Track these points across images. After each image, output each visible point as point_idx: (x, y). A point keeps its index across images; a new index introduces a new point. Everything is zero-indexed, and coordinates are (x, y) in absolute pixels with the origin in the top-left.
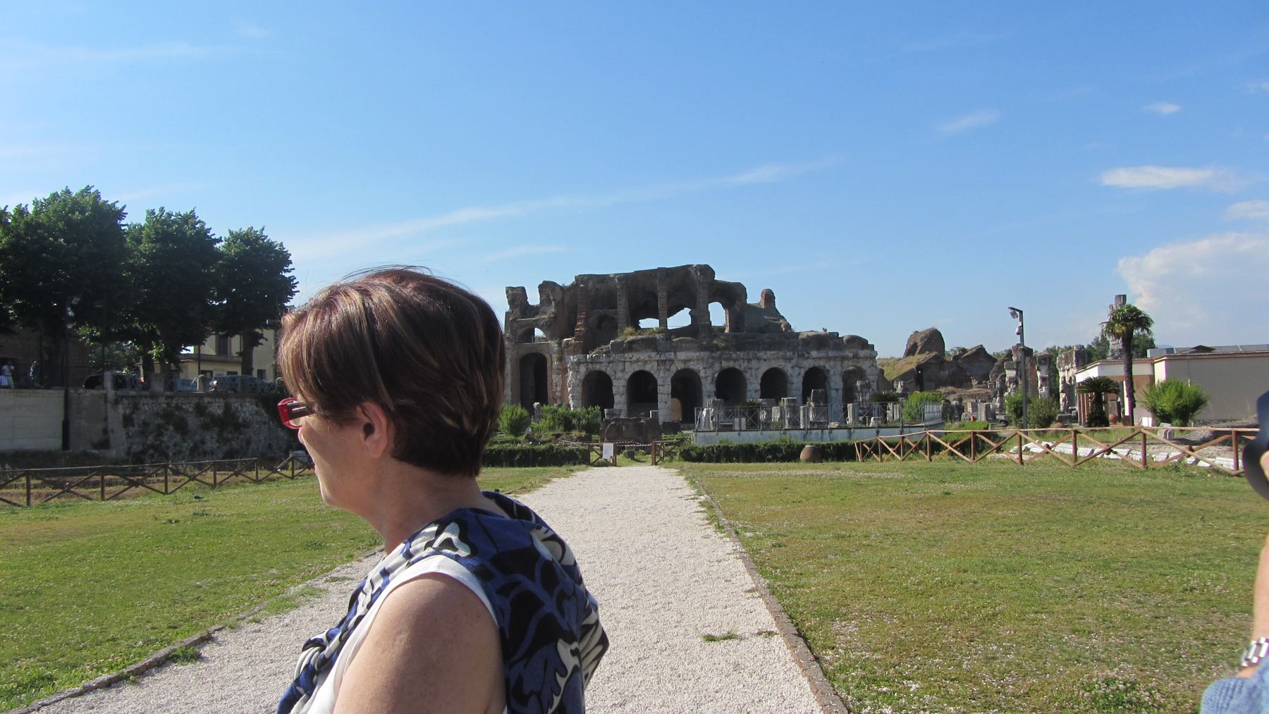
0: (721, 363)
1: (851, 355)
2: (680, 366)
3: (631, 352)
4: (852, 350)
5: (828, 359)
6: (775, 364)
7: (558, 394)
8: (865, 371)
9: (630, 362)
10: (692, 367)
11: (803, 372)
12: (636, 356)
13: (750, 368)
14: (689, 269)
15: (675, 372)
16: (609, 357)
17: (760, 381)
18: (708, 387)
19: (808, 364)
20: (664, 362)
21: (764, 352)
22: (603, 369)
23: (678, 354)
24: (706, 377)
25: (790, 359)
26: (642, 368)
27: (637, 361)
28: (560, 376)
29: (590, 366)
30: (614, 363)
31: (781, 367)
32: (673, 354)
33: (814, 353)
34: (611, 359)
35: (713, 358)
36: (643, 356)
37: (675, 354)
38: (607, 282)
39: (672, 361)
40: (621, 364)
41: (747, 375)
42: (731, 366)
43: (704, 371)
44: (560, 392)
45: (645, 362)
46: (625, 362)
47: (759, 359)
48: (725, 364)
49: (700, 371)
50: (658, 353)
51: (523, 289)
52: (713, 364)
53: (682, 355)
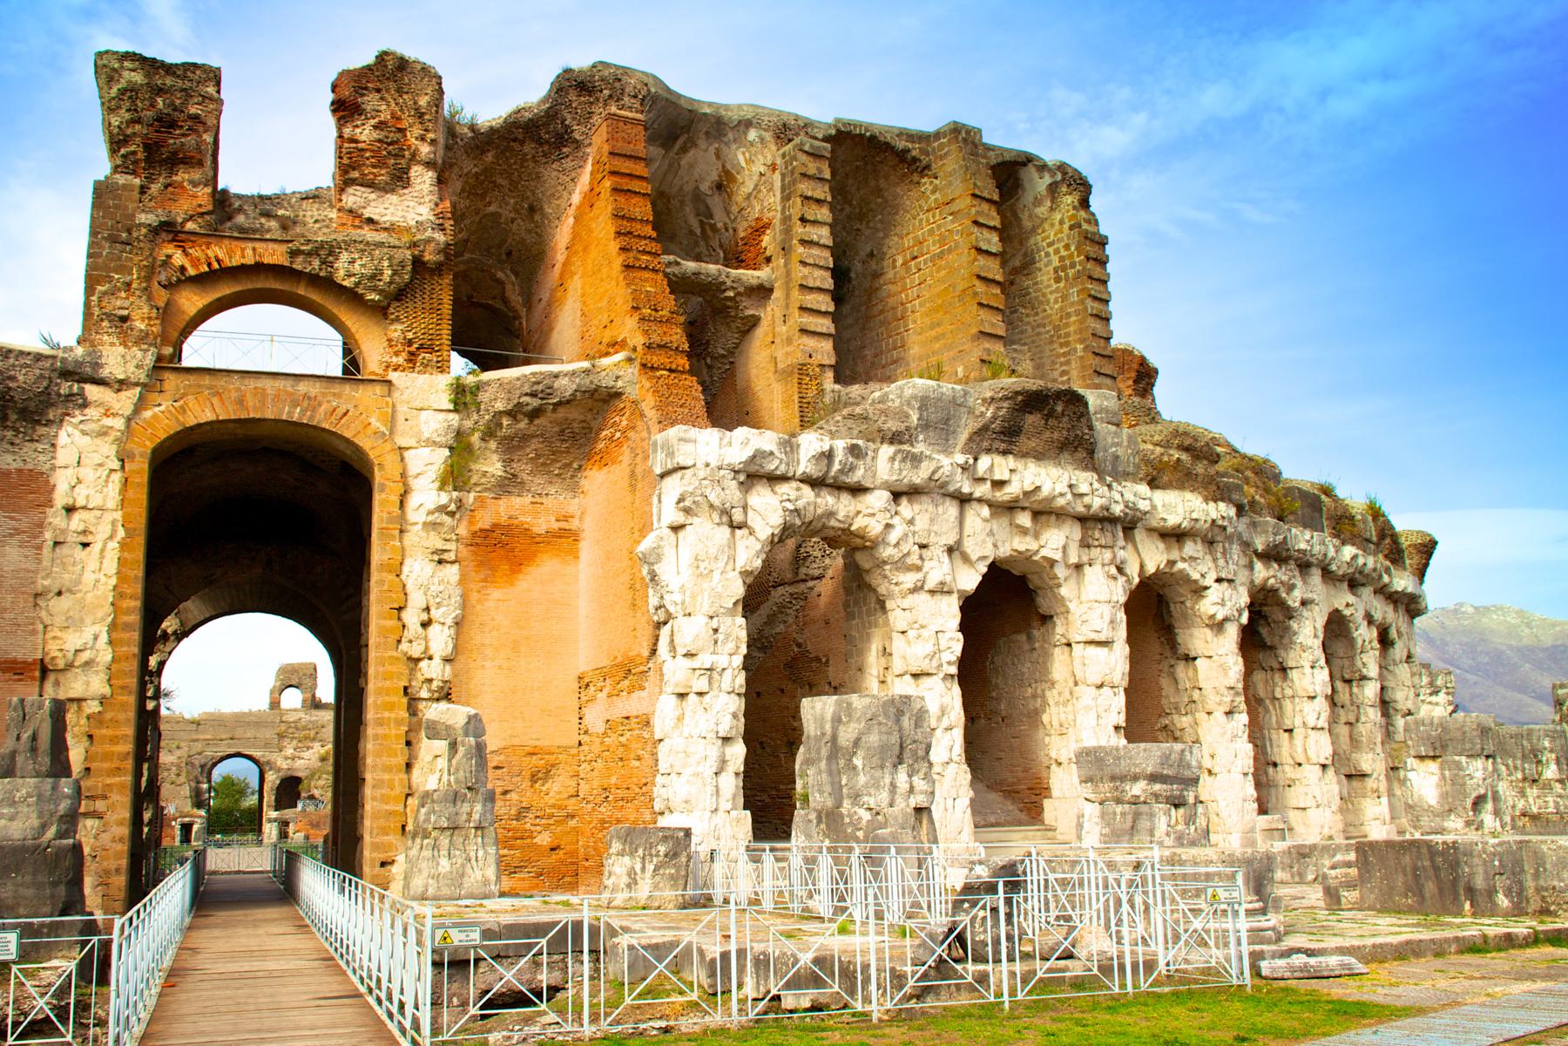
0: (1251, 567)
2: (1154, 557)
3: (1005, 453)
7: (433, 670)
20: (1104, 520)
22: (875, 528)
26: (1022, 544)
28: (452, 572)
31: (1347, 612)
34: (919, 476)
40: (951, 509)
44: (447, 660)
45: (1045, 513)
46: (964, 500)
51: (215, 76)
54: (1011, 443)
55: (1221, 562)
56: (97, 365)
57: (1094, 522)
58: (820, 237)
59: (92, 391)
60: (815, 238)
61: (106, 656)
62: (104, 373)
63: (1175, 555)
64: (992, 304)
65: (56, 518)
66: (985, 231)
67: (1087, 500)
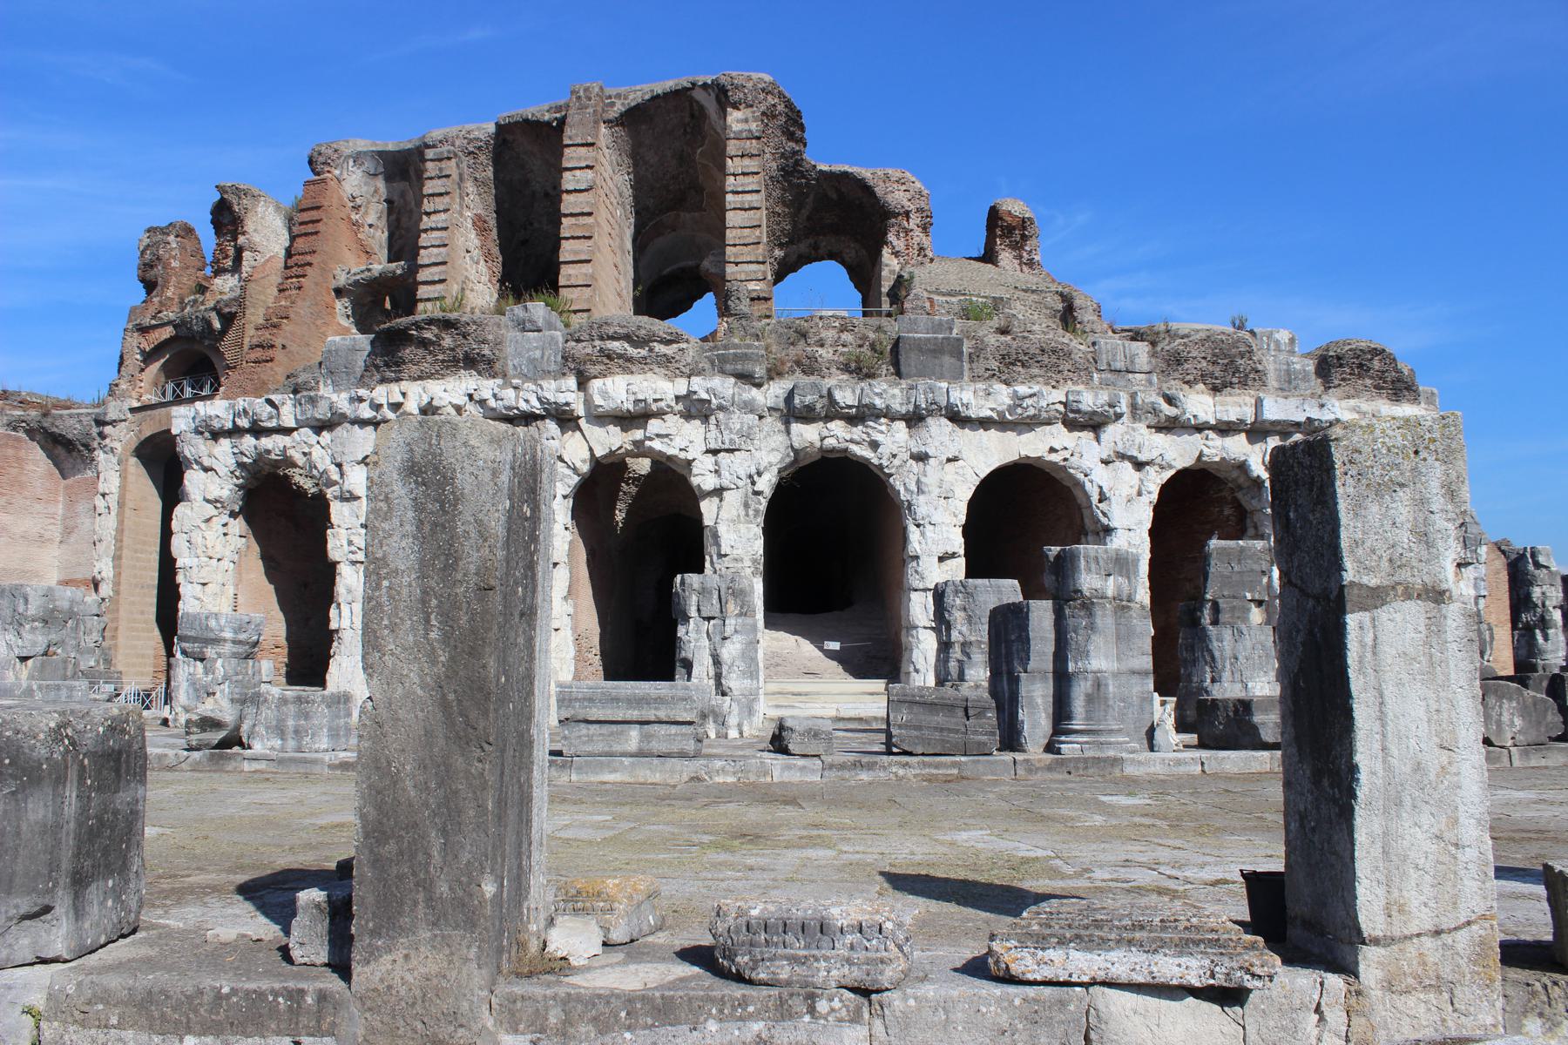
0: (788, 432)
2: (608, 440)
3: (398, 380)
4: (1352, 402)
11: (1155, 481)
13: (921, 458)
14: (699, 95)
15: (585, 468)
16: (313, 401)
17: (962, 519)
19: (1179, 452)
21: (981, 386)
23: (596, 384)
24: (719, 492)
25: (1094, 424)
29: (248, 442)
30: (339, 431)
31: (1054, 458)
32: (572, 382)
33: (1200, 404)
34: (322, 412)
35: (749, 407)
37: (582, 384)
41: (902, 483)
42: (830, 442)
43: (710, 459)
46: (375, 424)
47: (957, 418)
48: (808, 434)
49: (689, 463)
50: (507, 384)
52: (747, 435)
53: (616, 390)
54: (400, 372)
55: (714, 432)
56: (105, 414)
58: (438, 222)
59: (108, 429)
60: (434, 226)
61: (111, 575)
62: (108, 419)
63: (638, 434)
64: (576, 235)
66: (578, 173)
67: (492, 403)
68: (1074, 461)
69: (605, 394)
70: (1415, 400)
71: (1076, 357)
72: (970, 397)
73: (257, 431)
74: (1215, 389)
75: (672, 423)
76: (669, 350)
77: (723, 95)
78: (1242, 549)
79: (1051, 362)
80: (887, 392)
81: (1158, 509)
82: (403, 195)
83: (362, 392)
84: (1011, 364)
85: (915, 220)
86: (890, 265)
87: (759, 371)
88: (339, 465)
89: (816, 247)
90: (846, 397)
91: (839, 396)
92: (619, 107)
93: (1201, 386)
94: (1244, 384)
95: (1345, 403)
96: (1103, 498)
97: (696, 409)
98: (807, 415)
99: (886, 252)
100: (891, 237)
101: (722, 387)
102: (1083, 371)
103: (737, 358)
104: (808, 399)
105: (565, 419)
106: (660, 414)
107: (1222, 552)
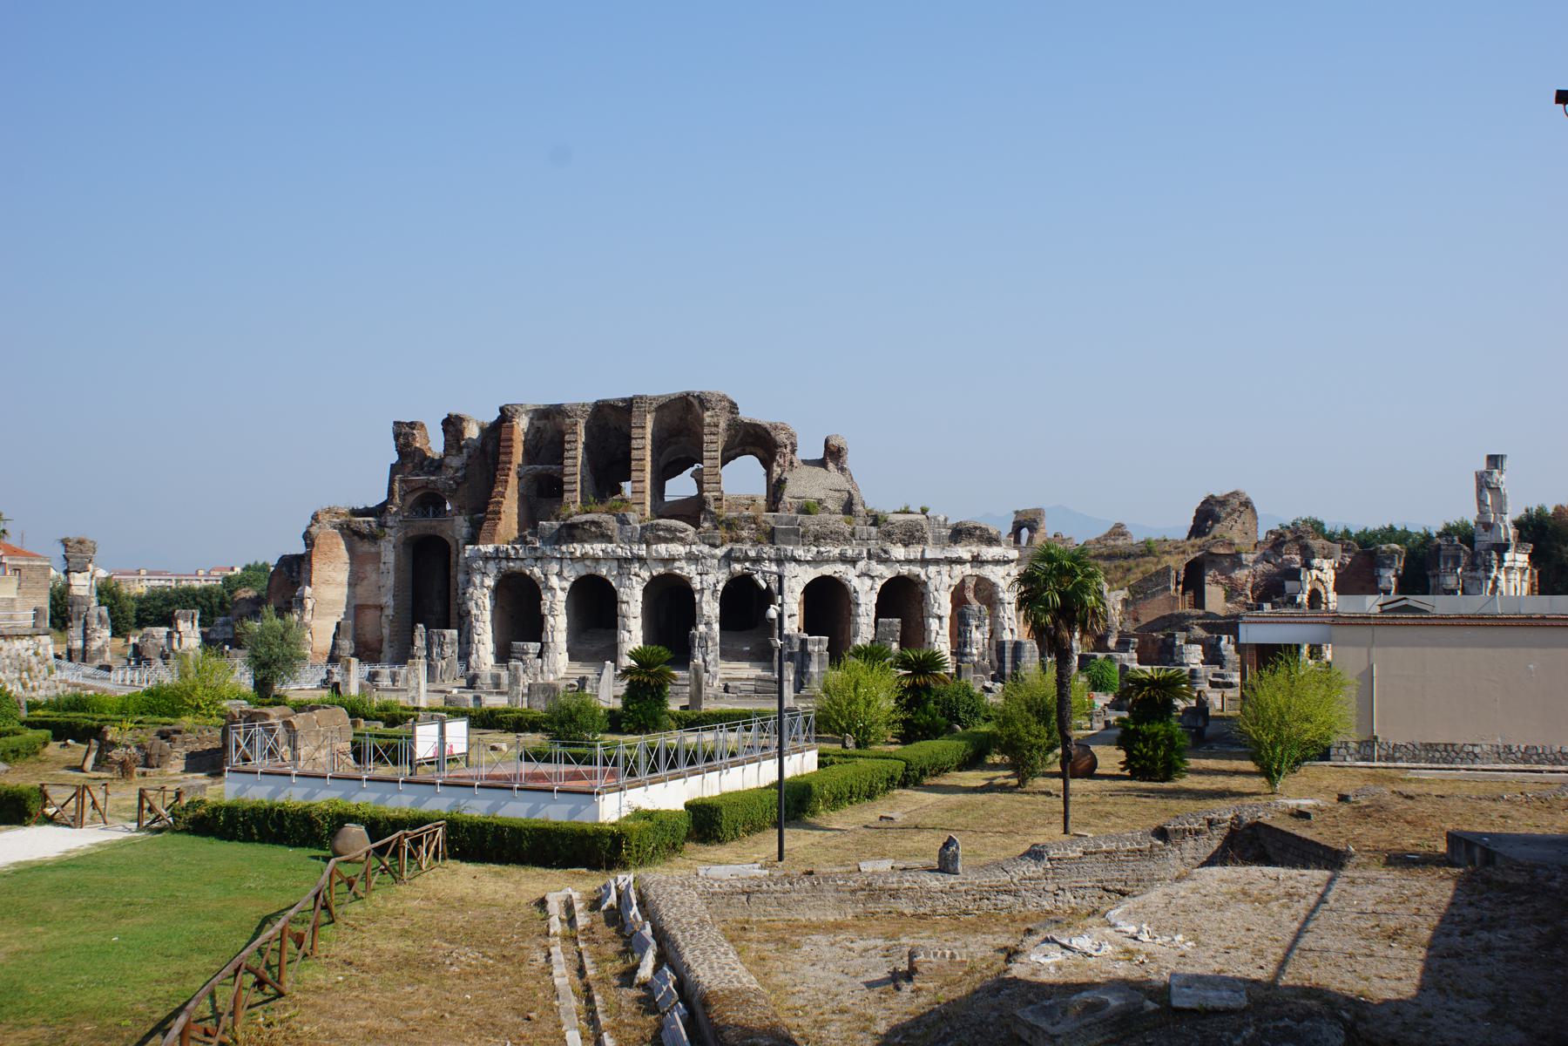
1: (967, 556)
4: (968, 548)
5: (924, 562)
6: (827, 570)
8: (994, 585)
9: (571, 559)
10: (678, 571)
11: (879, 584)
12: (578, 549)
18: (710, 608)
19: (888, 573)
24: (702, 590)
25: (853, 562)
26: (593, 571)
27: (584, 557)
29: (504, 563)
31: (837, 575)
32: (644, 546)
33: (898, 552)
35: (713, 557)
36: (596, 549)
38: (554, 418)
39: (641, 560)
43: (698, 577)
45: (596, 560)
49: (691, 578)
53: (662, 549)
55: (700, 567)
57: (623, 562)
59: (386, 529)
61: (392, 603)
65: (382, 566)
68: (844, 576)
69: (657, 551)
70: (1000, 545)
71: (847, 535)
72: (799, 552)
73: (508, 558)
74: (906, 546)
75: (683, 564)
76: (682, 535)
77: (703, 401)
78: (891, 622)
79: (835, 536)
80: (769, 551)
81: (879, 595)
82: (545, 425)
83: (557, 547)
84: (818, 539)
85: (789, 448)
86: (777, 470)
87: (718, 542)
88: (545, 575)
89: (744, 450)
90: (752, 554)
91: (749, 553)
92: (655, 405)
93: (899, 545)
94: (919, 543)
95: (964, 549)
96: (855, 592)
97: (692, 558)
98: (738, 560)
99: (775, 464)
100: (778, 458)
101: (706, 549)
102: (847, 541)
103: (710, 537)
104: (738, 555)
105: (641, 560)
106: (679, 560)
107: (882, 623)
